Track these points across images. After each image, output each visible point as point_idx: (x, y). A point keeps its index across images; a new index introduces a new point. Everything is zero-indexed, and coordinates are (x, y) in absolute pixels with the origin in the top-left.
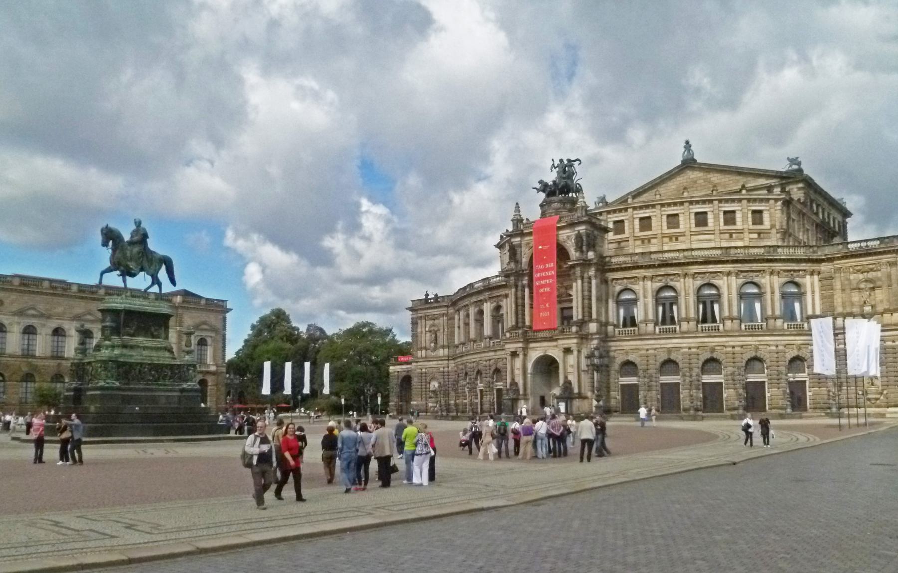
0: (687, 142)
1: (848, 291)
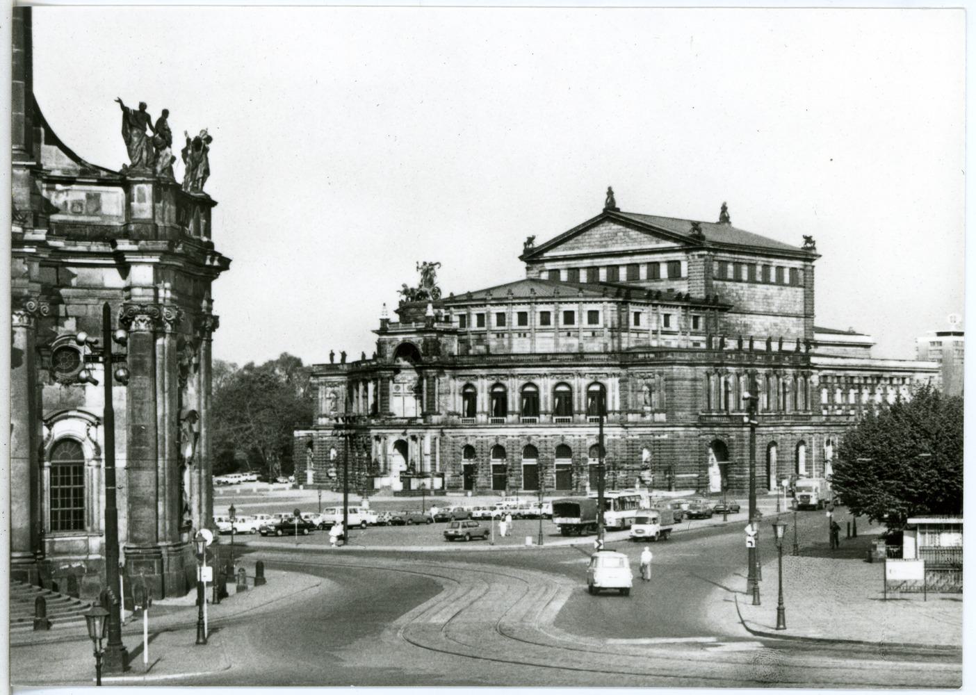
0: (610, 189)
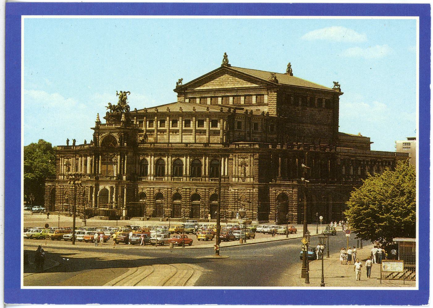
0: (225, 54)
1: (237, 166)
